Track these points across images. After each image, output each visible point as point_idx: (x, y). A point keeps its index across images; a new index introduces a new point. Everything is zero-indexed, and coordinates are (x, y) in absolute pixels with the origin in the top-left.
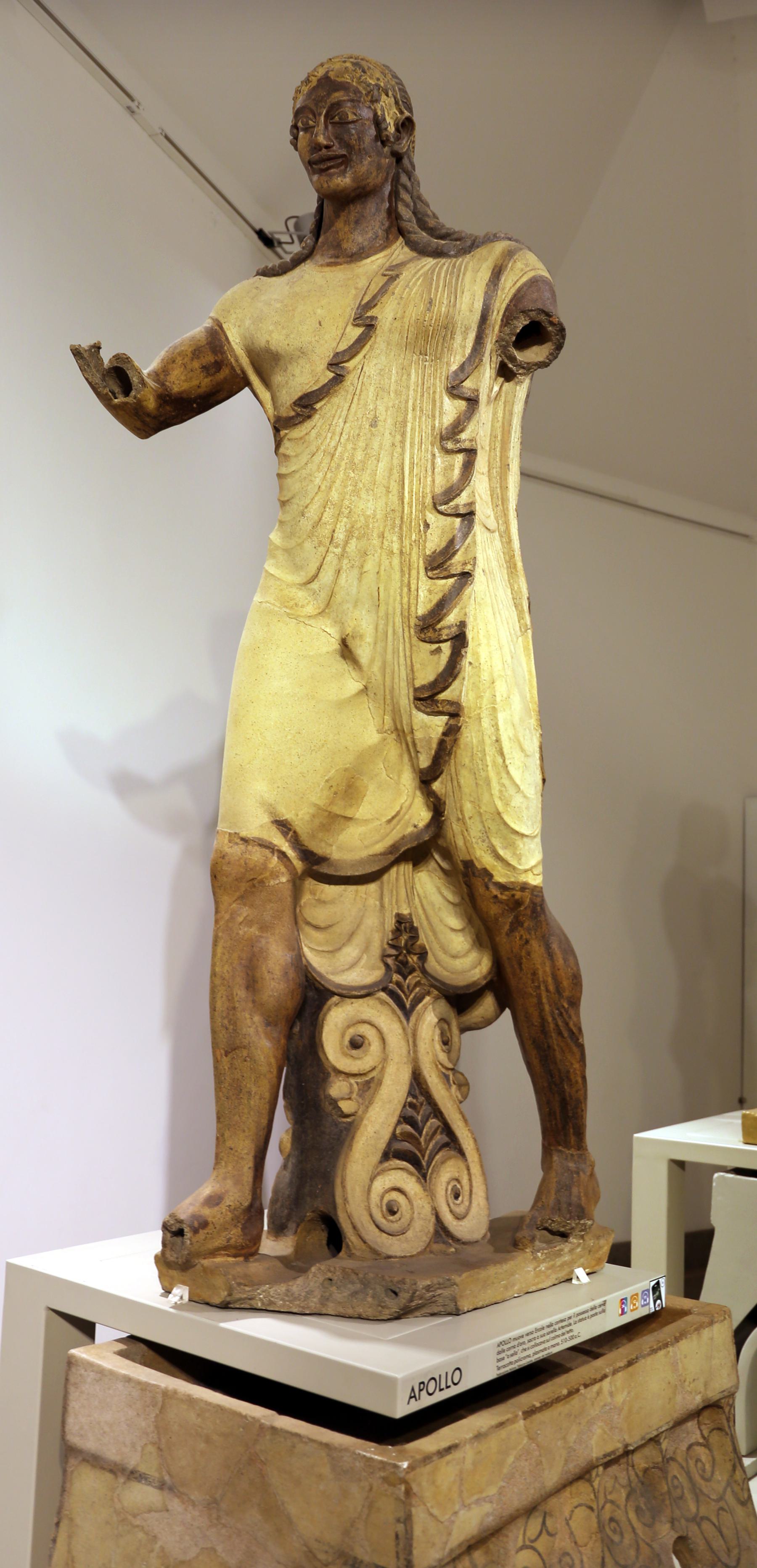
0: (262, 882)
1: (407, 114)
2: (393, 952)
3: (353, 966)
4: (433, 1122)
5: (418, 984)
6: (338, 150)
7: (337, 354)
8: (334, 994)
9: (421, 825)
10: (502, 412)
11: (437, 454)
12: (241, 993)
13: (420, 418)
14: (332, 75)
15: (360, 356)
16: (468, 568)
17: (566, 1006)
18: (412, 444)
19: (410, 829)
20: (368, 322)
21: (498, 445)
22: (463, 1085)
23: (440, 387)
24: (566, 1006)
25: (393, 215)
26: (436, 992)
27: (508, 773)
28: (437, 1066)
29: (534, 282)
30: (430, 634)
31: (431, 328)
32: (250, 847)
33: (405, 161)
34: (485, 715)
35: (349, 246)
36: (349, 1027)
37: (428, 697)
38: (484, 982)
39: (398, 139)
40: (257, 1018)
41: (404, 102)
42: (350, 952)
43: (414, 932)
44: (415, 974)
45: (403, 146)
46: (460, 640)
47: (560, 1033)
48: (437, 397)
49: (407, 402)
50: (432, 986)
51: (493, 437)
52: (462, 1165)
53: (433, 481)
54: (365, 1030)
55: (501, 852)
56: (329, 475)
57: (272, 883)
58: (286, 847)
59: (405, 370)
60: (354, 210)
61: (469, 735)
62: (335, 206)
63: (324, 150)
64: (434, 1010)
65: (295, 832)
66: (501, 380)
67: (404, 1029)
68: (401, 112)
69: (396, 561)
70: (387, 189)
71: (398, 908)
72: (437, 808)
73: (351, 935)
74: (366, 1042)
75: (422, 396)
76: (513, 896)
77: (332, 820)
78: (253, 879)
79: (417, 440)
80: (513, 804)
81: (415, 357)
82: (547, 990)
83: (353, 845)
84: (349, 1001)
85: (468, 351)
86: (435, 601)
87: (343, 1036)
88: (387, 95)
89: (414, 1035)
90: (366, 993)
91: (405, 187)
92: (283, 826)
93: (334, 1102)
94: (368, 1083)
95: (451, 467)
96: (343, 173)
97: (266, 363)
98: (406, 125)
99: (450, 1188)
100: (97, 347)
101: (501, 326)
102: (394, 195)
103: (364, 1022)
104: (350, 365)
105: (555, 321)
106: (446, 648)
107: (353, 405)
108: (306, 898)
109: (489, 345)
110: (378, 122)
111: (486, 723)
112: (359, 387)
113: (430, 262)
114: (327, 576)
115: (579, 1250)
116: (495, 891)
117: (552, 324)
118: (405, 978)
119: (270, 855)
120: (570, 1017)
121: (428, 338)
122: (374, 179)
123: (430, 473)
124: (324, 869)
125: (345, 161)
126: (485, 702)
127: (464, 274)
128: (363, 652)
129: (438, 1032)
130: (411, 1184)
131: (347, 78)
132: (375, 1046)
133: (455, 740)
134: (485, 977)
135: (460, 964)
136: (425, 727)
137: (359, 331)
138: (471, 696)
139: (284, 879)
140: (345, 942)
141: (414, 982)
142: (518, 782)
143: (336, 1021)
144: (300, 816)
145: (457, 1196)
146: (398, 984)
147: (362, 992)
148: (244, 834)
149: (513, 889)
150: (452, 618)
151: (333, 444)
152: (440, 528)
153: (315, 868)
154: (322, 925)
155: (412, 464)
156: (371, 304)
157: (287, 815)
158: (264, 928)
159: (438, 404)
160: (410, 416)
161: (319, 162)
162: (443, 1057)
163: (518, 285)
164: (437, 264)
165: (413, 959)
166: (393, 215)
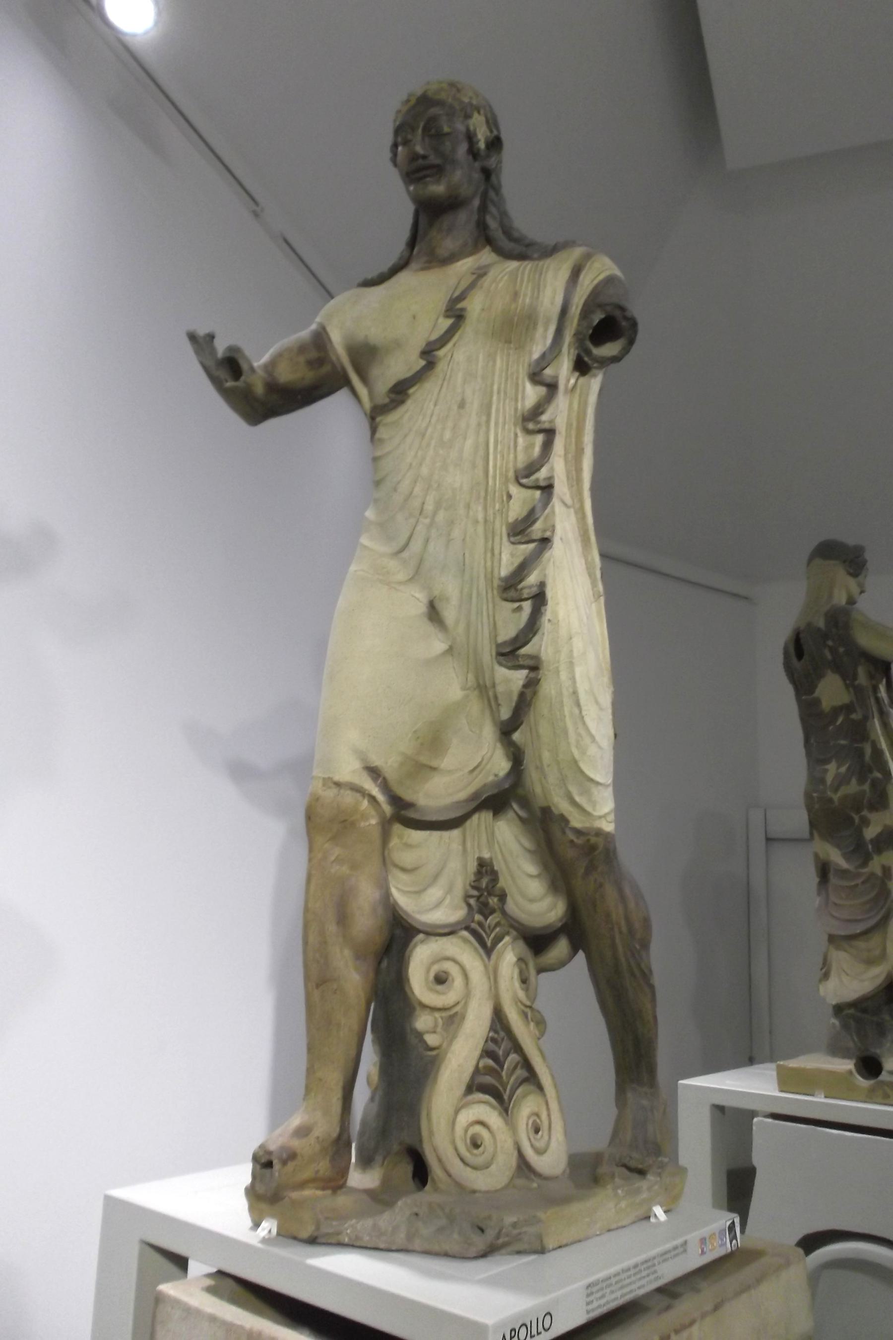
0: (353, 824)
1: (495, 133)
2: (475, 893)
3: (438, 905)
4: (513, 1057)
5: (498, 924)
6: (434, 160)
7: (429, 344)
8: (419, 931)
9: (502, 774)
10: (577, 404)
11: (519, 434)
12: (332, 928)
13: (504, 400)
14: (430, 94)
15: (450, 345)
16: (548, 534)
17: (638, 947)
18: (496, 424)
19: (491, 778)
20: (458, 313)
21: (573, 433)
22: (541, 1023)
23: (523, 373)
24: (638, 947)
25: (482, 226)
26: (514, 933)
27: (584, 723)
28: (516, 1003)
29: (610, 280)
30: (512, 594)
31: (516, 319)
32: (342, 791)
33: (493, 178)
34: (563, 668)
35: (442, 252)
36: (433, 963)
37: (509, 653)
38: (560, 924)
39: (488, 156)
40: (347, 952)
41: (492, 122)
42: (435, 893)
43: (494, 876)
44: (495, 915)
45: (492, 162)
46: (539, 598)
47: (633, 975)
48: (520, 382)
49: (492, 385)
50: (512, 926)
51: (569, 425)
52: (540, 1099)
53: (516, 457)
54: (448, 966)
55: (578, 799)
56: (420, 453)
57: (362, 824)
58: (376, 791)
59: (491, 357)
60: (446, 220)
61: (547, 688)
62: (431, 212)
63: (421, 161)
64: (513, 950)
65: (384, 779)
66: (577, 374)
67: (486, 967)
68: (491, 131)
69: (480, 529)
70: (476, 202)
71: (480, 851)
72: (517, 757)
73: (436, 877)
74: (450, 978)
75: (507, 380)
76: (588, 840)
77: (420, 769)
78: (345, 821)
79: (501, 420)
80: (589, 753)
81: (500, 345)
82: (621, 933)
83: (438, 793)
84: (433, 938)
85: (549, 341)
86: (516, 564)
87: (428, 971)
88: (479, 112)
90: (450, 931)
91: (492, 201)
92: (374, 772)
93: (420, 1035)
94: (452, 1018)
95: (532, 446)
96: (438, 182)
97: (364, 355)
98: (495, 144)
100: (211, 337)
101: (579, 320)
102: (483, 209)
103: (447, 959)
104: (441, 353)
105: (628, 314)
106: (527, 606)
107: (444, 390)
108: (394, 842)
109: (568, 337)
110: (470, 137)
111: (564, 676)
112: (448, 374)
113: (513, 265)
114: (416, 546)
116: (571, 836)
117: (626, 318)
118: (486, 919)
119: (360, 798)
121: (513, 328)
122: (465, 191)
123: (512, 451)
124: (412, 814)
125: (438, 171)
126: (563, 657)
127: (546, 272)
128: (450, 614)
131: (443, 96)
133: (535, 693)
134: (561, 920)
135: (536, 908)
136: (508, 681)
137: (449, 322)
138: (550, 651)
139: (373, 821)
140: (430, 882)
141: (494, 922)
142: (593, 732)
143: (421, 958)
144: (389, 764)
146: (480, 924)
147: (446, 930)
148: (337, 778)
149: (588, 834)
150: (532, 579)
151: (424, 425)
152: (521, 500)
153: (403, 812)
154: (409, 867)
155: (496, 442)
156: (462, 297)
157: (377, 761)
158: (354, 866)
159: (520, 388)
160: (495, 398)
161: (416, 171)
162: (521, 994)
163: (596, 282)
164: (520, 267)
165: (493, 901)
166: (482, 226)
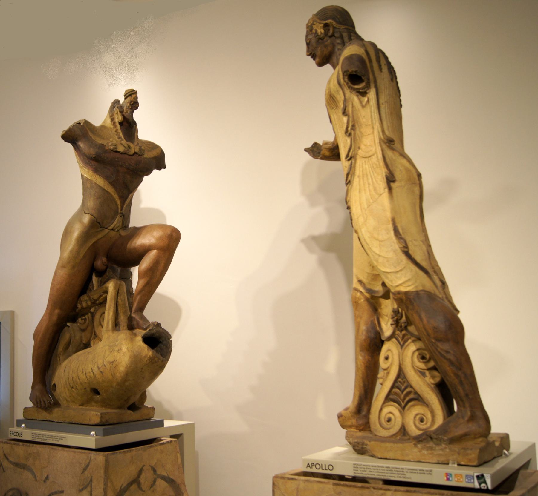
24: (434, 341)
89: (402, 354)
99: (418, 417)
115: (447, 450)
120: (438, 346)
129: (417, 353)
130: (397, 413)
139: (362, 300)
142: (378, 252)
145: (422, 420)
157: (361, 278)
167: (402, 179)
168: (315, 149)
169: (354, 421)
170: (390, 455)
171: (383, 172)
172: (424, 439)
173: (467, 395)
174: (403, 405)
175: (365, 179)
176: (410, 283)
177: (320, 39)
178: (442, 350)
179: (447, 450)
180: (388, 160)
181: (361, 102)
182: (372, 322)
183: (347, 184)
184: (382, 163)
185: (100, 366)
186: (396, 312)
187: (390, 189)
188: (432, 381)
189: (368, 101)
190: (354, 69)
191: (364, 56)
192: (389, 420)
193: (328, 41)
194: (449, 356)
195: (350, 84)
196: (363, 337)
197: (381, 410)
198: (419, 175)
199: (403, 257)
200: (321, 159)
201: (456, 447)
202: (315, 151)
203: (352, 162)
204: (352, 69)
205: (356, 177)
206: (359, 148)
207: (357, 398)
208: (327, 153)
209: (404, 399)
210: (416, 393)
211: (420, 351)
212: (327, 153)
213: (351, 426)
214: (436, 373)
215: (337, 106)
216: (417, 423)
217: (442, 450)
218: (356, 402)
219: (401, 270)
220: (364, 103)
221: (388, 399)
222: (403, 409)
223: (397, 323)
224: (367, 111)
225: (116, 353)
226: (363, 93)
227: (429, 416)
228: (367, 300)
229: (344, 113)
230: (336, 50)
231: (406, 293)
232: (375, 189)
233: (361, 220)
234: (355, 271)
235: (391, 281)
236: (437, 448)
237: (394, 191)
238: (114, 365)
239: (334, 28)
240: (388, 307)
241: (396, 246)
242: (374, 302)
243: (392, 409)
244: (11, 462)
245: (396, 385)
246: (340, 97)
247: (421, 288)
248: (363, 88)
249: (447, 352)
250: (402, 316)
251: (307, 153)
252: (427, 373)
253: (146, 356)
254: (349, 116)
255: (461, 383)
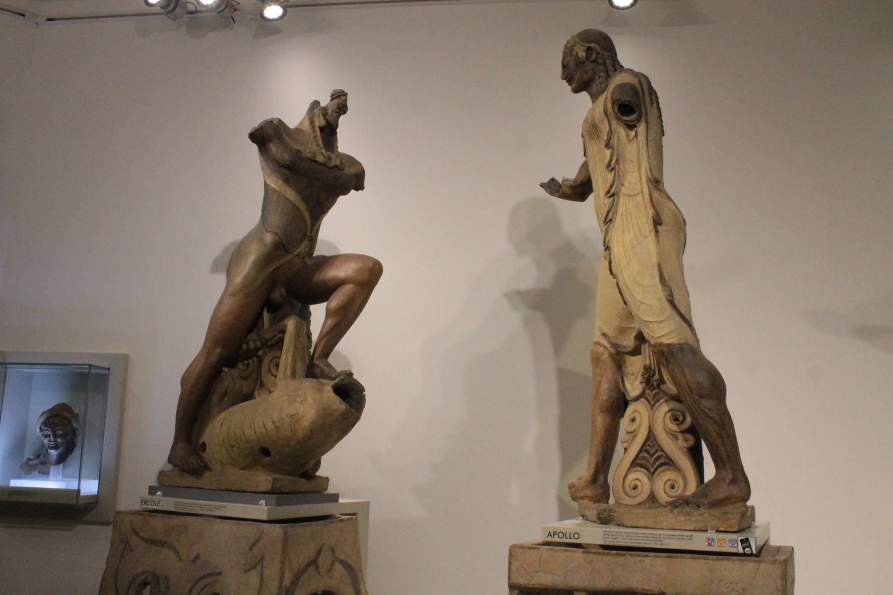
58: (605, 343)
99: (668, 483)
115: (707, 515)
129: (669, 414)
132: (638, 421)
145: (673, 487)
157: (606, 331)
167: (666, 222)
168: (552, 185)
169: (588, 492)
170: (642, 523)
171: (651, 212)
172: (681, 504)
173: (729, 457)
174: (652, 470)
175: (629, 218)
176: (673, 335)
177: (580, 63)
178: (705, 407)
179: (707, 515)
180: (654, 200)
181: (628, 136)
182: (616, 382)
183: (605, 222)
184: (649, 204)
185: (275, 420)
186: (647, 369)
187: (657, 232)
188: (685, 445)
189: (636, 135)
190: (628, 99)
191: (638, 86)
192: (635, 488)
193: (589, 66)
194: (712, 414)
195: (619, 114)
196: (604, 396)
197: (626, 476)
198: (684, 221)
199: (668, 306)
200: (560, 197)
201: (716, 512)
202: (552, 187)
203: (614, 200)
204: (625, 98)
205: (618, 216)
206: (622, 185)
207: (593, 465)
208: (568, 192)
209: (654, 464)
210: (667, 457)
211: (673, 412)
212: (568, 192)
213: (583, 498)
214: (690, 437)
215: (599, 137)
216: (668, 489)
217: (700, 516)
218: (592, 470)
219: (665, 320)
220: (631, 138)
221: (634, 464)
222: (652, 474)
223: (648, 381)
224: (633, 147)
225: (298, 405)
226: (630, 126)
227: (681, 482)
228: (611, 355)
229: (608, 145)
230: (597, 77)
231: (668, 345)
232: (640, 231)
233: (624, 263)
234: (598, 323)
235: (653, 331)
236: (696, 513)
237: (660, 235)
238: (296, 419)
239: (598, 53)
240: (636, 365)
241: (660, 293)
242: (619, 358)
243: (640, 475)
244: (142, 538)
245: (645, 448)
246: (604, 128)
247: (684, 341)
248: (632, 121)
249: (710, 410)
250: (655, 374)
251: (542, 189)
252: (680, 436)
253: (337, 410)
254: (613, 150)
255: (724, 443)
